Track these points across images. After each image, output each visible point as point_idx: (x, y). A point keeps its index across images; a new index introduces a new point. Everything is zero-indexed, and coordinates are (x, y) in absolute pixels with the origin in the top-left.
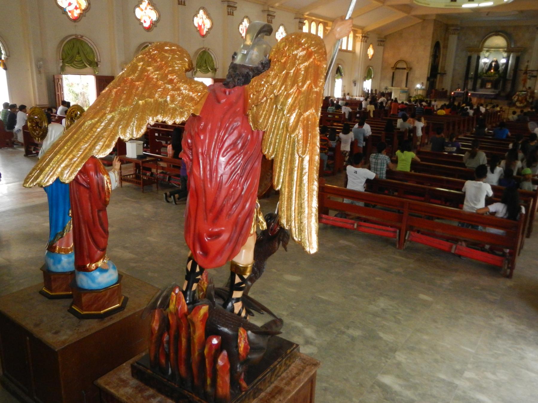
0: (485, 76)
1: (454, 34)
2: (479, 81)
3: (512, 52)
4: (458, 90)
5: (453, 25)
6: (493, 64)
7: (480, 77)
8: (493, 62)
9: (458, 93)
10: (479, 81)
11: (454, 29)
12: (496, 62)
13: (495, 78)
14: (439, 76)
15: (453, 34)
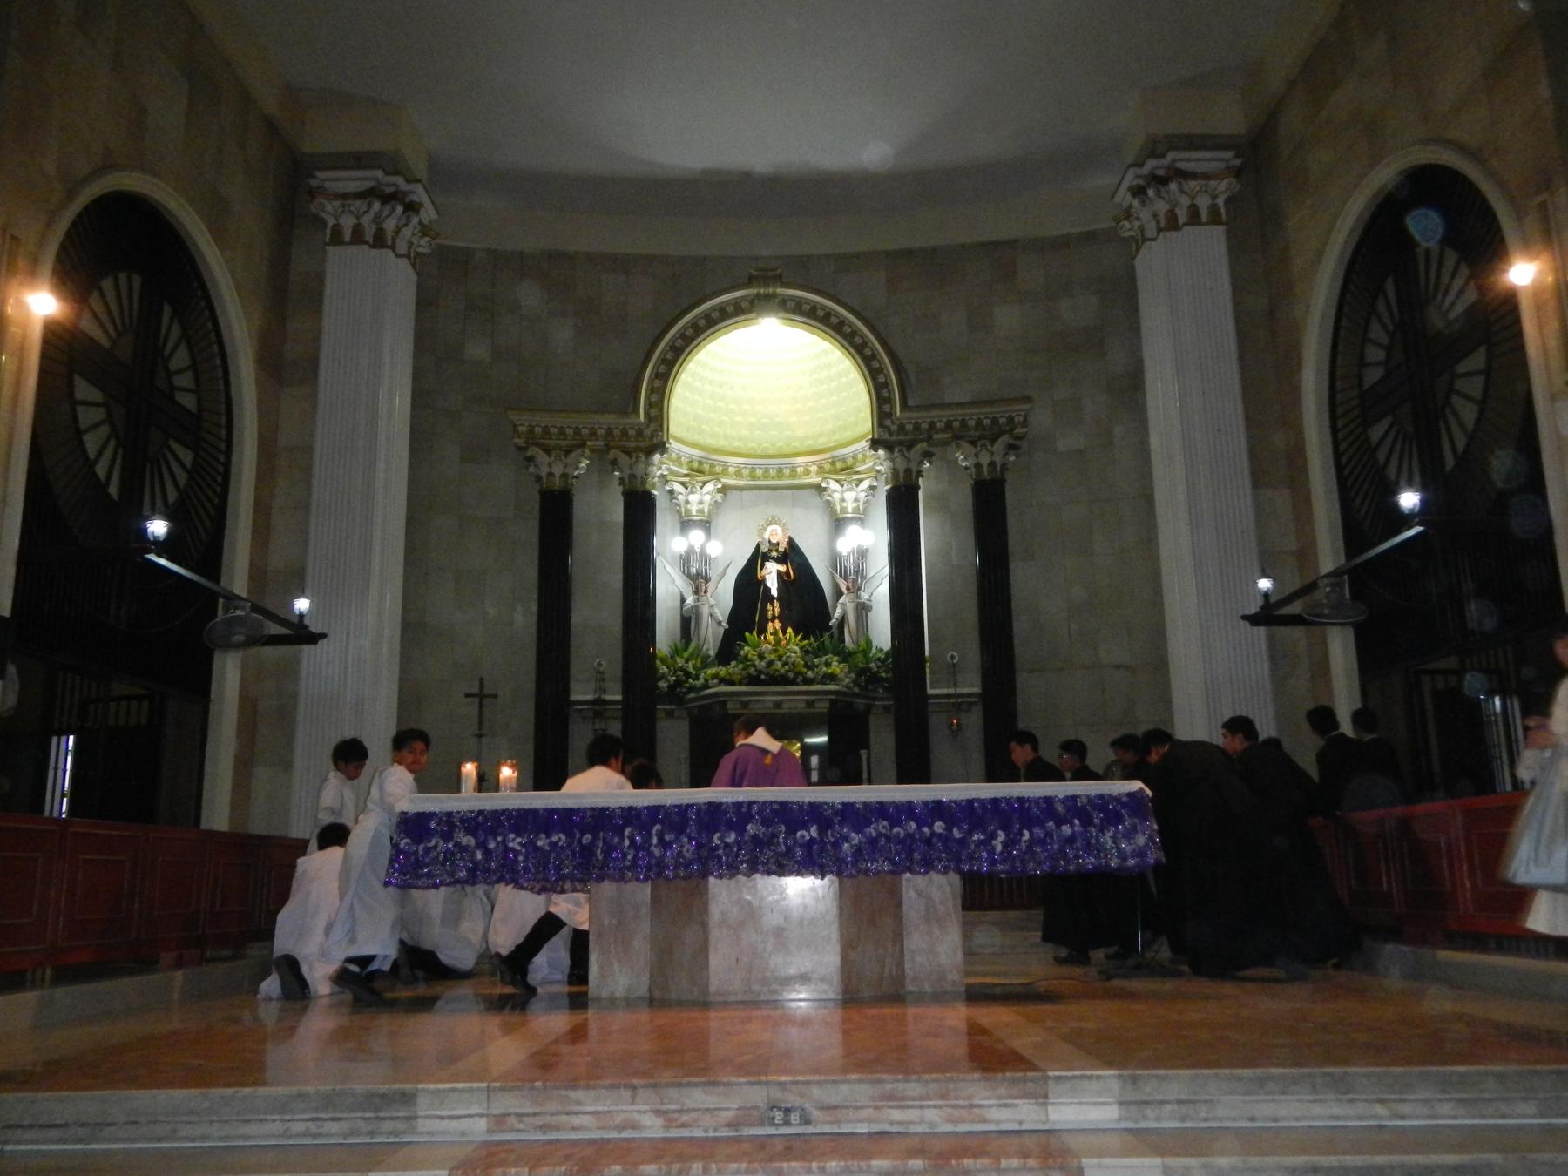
0: (723, 681)
1: (379, 241)
2: (673, 736)
3: (928, 455)
4: (486, 781)
5: (359, 160)
6: (771, 574)
7: (676, 694)
8: (758, 557)
9: (484, 824)
10: (673, 736)
11: (361, 195)
12: (792, 554)
13: (832, 687)
14: (229, 672)
15: (358, 237)
